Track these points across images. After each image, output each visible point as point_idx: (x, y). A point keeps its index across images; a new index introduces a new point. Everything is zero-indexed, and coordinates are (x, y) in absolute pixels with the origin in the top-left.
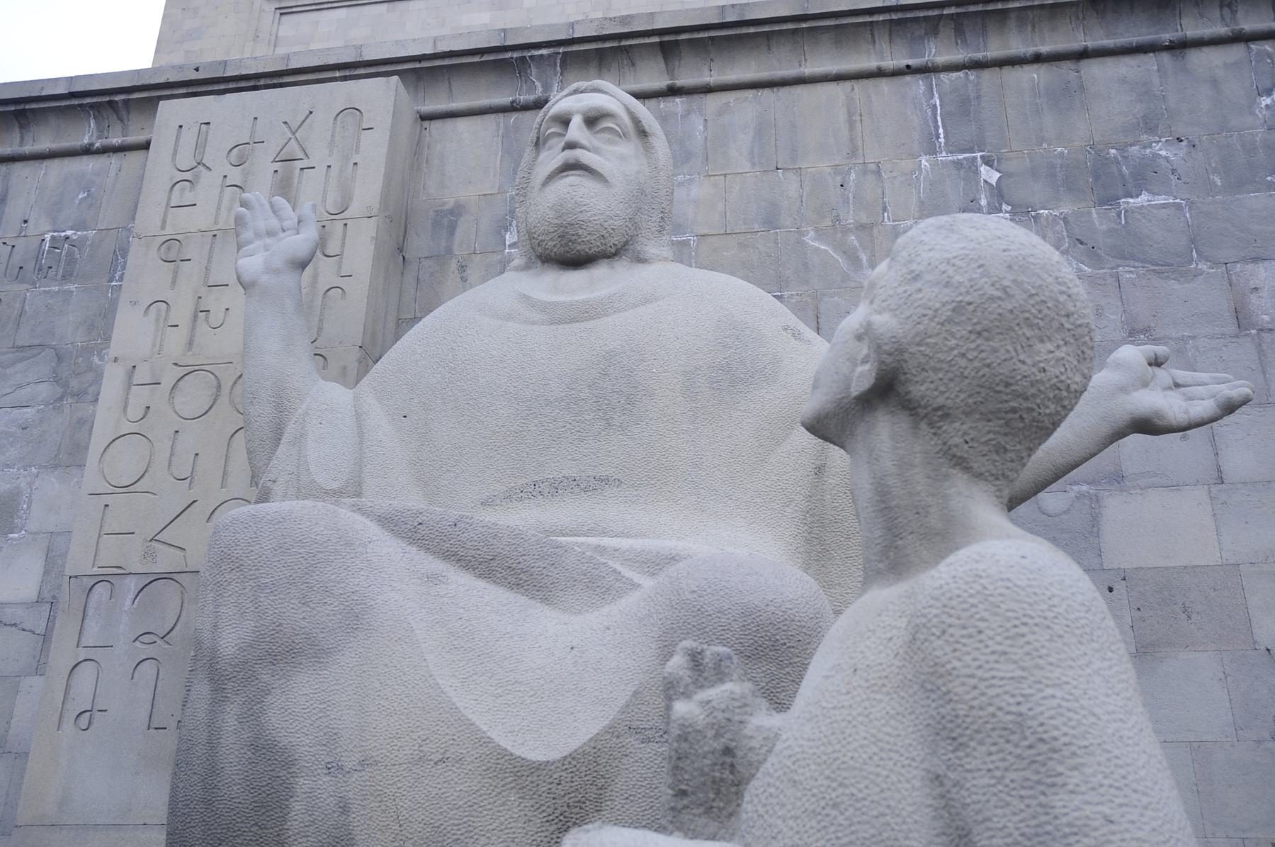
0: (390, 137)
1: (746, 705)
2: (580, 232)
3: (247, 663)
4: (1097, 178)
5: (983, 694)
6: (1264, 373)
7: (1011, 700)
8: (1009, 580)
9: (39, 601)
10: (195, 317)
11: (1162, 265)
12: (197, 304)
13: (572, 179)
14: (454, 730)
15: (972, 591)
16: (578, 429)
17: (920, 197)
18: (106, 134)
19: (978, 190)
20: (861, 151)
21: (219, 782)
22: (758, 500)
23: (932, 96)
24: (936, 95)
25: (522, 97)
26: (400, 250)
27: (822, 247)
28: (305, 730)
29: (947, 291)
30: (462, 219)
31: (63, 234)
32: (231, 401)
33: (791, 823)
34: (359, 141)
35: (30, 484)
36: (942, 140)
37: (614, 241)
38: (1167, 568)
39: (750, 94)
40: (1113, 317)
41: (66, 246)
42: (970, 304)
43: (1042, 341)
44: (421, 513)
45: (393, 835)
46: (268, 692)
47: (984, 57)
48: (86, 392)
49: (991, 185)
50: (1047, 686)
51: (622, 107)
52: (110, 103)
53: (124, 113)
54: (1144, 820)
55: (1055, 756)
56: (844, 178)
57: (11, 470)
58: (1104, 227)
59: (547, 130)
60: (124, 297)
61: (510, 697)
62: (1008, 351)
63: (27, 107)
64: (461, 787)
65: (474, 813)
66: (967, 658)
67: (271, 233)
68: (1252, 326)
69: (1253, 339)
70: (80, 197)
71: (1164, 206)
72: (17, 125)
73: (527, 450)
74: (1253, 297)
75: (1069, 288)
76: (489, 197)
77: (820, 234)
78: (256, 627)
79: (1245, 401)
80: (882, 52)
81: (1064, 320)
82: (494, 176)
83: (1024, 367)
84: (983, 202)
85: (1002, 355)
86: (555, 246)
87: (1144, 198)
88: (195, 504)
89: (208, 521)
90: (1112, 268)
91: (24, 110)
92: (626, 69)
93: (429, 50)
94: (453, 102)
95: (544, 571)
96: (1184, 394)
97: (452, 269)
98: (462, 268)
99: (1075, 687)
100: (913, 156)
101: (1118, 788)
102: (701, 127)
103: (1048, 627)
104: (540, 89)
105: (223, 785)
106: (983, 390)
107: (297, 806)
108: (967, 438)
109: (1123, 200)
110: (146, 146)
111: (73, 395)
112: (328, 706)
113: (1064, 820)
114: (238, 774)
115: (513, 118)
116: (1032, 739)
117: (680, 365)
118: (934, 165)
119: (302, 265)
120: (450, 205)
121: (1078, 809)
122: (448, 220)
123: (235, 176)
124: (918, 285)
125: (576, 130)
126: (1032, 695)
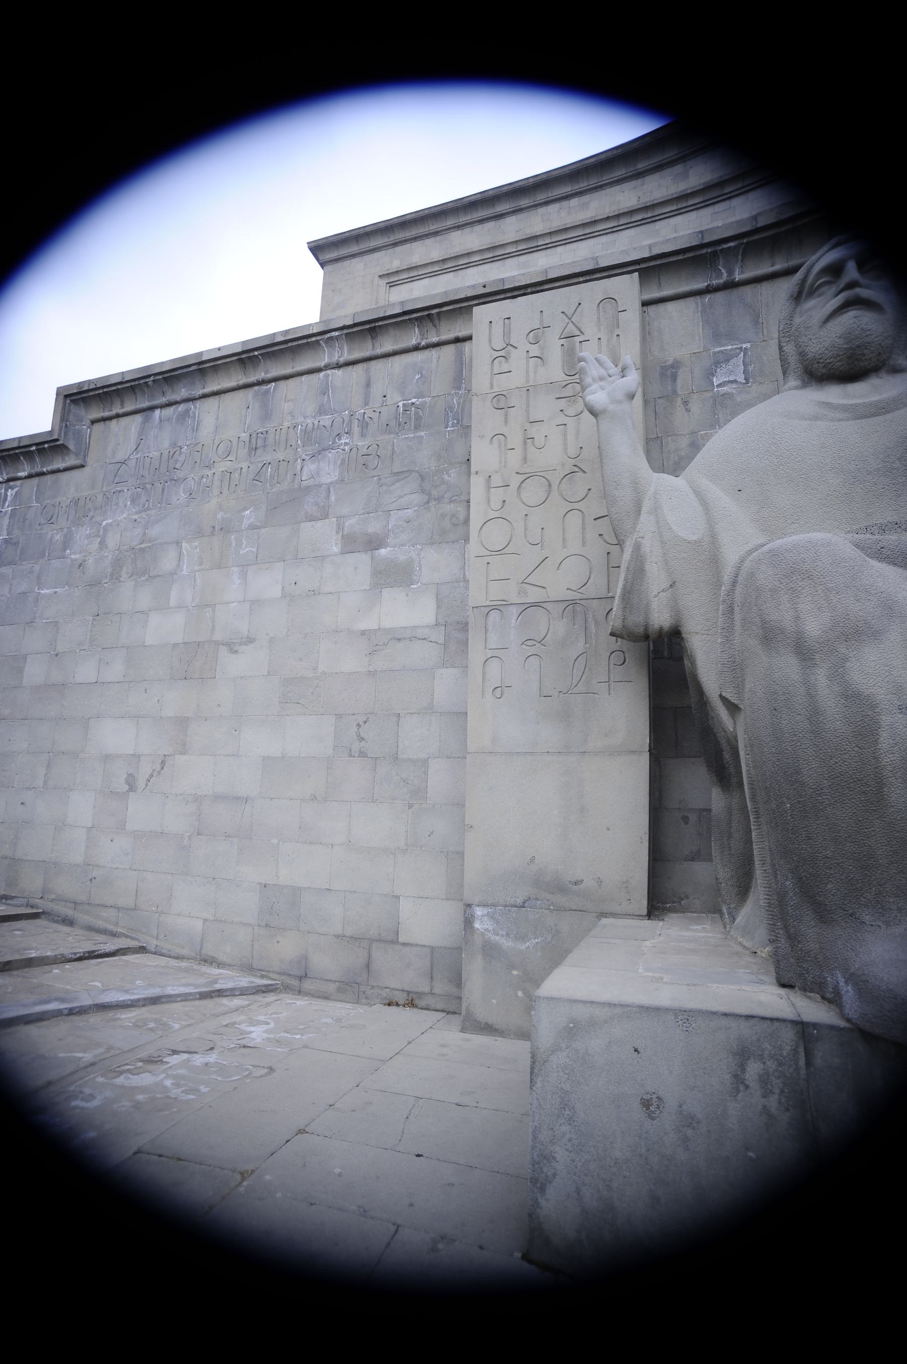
3: (829, 641)
10: (525, 443)
16: (895, 489)
18: (426, 336)
21: (823, 719)
32: (561, 494)
35: (418, 555)
41: (413, 409)
44: (880, 541)
46: (846, 659)
48: (443, 497)
52: (429, 315)
53: (437, 321)
63: (377, 324)
67: (601, 379)
70: (416, 377)
72: (370, 337)
73: (857, 505)
76: (698, 354)
78: (832, 616)
82: (699, 340)
89: (558, 569)
91: (375, 327)
93: (646, 254)
94: (662, 291)
97: (678, 404)
98: (686, 403)
105: (828, 721)
110: (470, 338)
111: (435, 500)
112: (891, 668)
114: (838, 714)
115: (707, 298)
120: (671, 362)
123: (535, 350)
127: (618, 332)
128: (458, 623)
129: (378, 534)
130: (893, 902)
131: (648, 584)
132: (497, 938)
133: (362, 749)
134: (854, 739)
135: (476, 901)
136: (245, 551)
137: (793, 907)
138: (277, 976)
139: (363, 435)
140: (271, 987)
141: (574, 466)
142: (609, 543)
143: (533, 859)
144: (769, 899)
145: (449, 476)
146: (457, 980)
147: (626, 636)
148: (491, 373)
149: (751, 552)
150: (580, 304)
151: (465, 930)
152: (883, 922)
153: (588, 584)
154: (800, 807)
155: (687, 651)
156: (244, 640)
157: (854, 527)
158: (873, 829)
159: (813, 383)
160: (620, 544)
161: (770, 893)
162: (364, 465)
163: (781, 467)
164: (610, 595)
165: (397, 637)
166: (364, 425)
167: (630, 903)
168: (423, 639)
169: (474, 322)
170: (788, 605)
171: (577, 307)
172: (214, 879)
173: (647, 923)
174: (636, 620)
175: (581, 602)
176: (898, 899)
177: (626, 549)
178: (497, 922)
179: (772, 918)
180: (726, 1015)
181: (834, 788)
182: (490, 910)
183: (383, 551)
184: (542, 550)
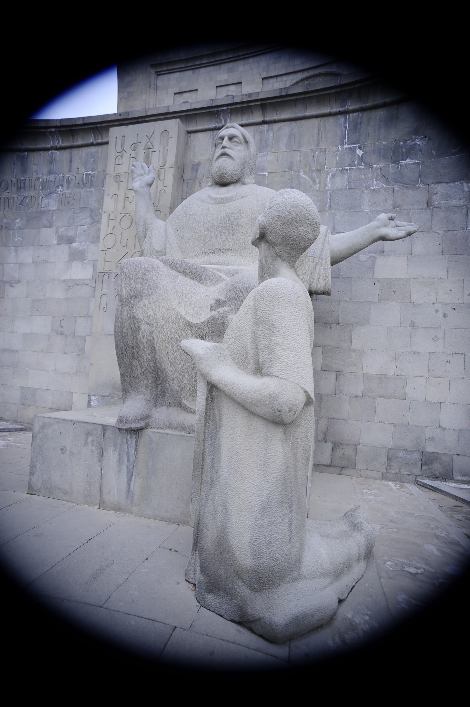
0: (177, 140)
1: (228, 313)
2: (225, 176)
5: (263, 314)
6: (431, 221)
7: (268, 316)
8: (272, 288)
10: (125, 199)
11: (408, 185)
12: (125, 195)
13: (224, 158)
15: (264, 290)
17: (337, 160)
20: (320, 144)
25: (218, 125)
26: (182, 177)
28: (142, 314)
29: (277, 212)
30: (200, 167)
31: (89, 173)
33: (230, 340)
34: (168, 142)
35: (87, 247)
36: (346, 140)
37: (236, 178)
38: (391, 279)
39: (288, 123)
40: (389, 202)
41: (90, 176)
42: (281, 216)
43: (300, 226)
50: (276, 313)
51: (240, 133)
54: (291, 343)
55: (275, 328)
56: (314, 154)
58: (393, 171)
59: (218, 141)
60: (106, 194)
61: (190, 307)
62: (290, 229)
66: (261, 305)
67: (141, 175)
69: (431, 210)
70: (92, 160)
74: (434, 196)
75: (310, 212)
77: (305, 173)
79: (415, 232)
81: (307, 221)
83: (295, 233)
84: (356, 162)
85: (289, 230)
86: (218, 180)
96: (398, 229)
98: (200, 183)
99: (282, 314)
101: (286, 336)
102: (272, 136)
103: (279, 300)
106: (284, 239)
107: (141, 332)
108: (281, 251)
109: (401, 162)
113: (274, 342)
116: (270, 324)
117: (251, 217)
118: (343, 149)
119: (150, 185)
120: (196, 162)
121: (277, 340)
122: (196, 167)
123: (133, 154)
124: (271, 210)
125: (226, 142)
126: (272, 315)
127: (167, 148)
135: (92, 394)
136: (17, 240)
138: (26, 425)
139: (68, 188)
140: (24, 429)
148: (115, 164)
156: (16, 281)
166: (69, 182)
172: (3, 385)
180: (84, 422)
182: (97, 398)
183: (74, 245)
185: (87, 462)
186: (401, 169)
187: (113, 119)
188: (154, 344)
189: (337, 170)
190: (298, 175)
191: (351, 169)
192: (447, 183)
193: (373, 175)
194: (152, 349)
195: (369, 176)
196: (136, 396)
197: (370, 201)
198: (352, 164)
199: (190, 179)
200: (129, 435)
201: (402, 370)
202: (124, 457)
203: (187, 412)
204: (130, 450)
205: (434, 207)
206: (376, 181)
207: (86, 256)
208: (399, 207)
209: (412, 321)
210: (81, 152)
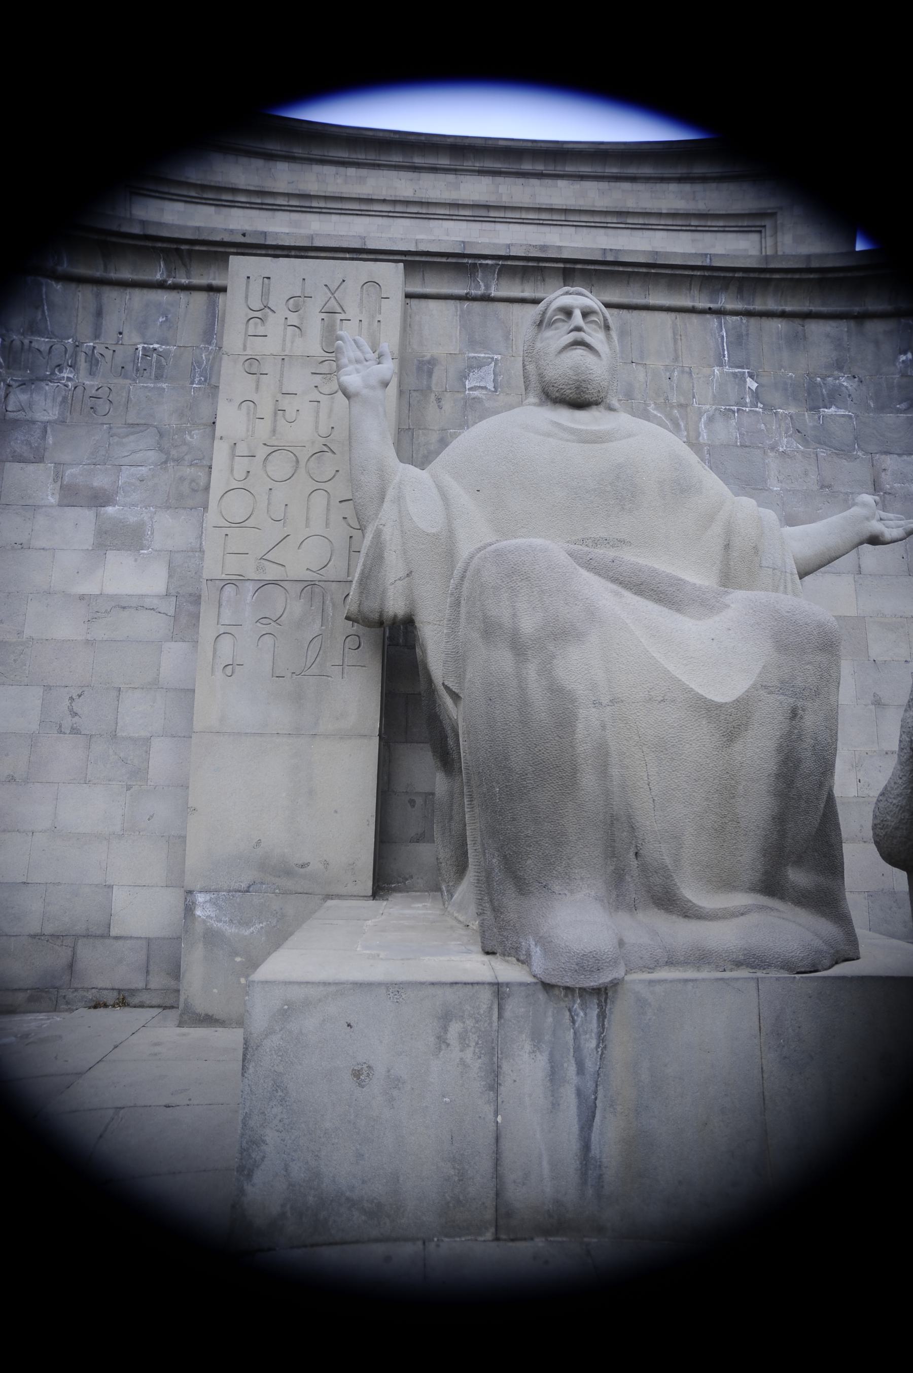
2: (589, 386)
4: (809, 394)
9: (168, 595)
10: (275, 414)
13: (579, 352)
14: (669, 684)
19: (745, 393)
20: (680, 358)
22: (700, 561)
23: (721, 330)
24: (724, 330)
27: (659, 415)
28: (579, 681)
30: (437, 368)
31: (151, 346)
32: (308, 473)
35: (151, 518)
40: (813, 477)
45: (635, 743)
46: (553, 657)
47: (754, 309)
48: (183, 459)
49: (752, 390)
56: (671, 374)
57: (136, 508)
64: (675, 716)
65: (683, 731)
67: (358, 361)
68: (881, 490)
70: (161, 320)
71: (843, 416)
73: (577, 519)
74: (883, 474)
77: (658, 407)
80: (694, 297)
82: (456, 342)
84: (748, 400)
87: (832, 410)
88: (288, 537)
89: (299, 548)
90: (814, 449)
92: (539, 283)
95: (673, 594)
96: (884, 524)
97: (432, 400)
98: (439, 400)
100: (710, 366)
104: (483, 288)
107: (580, 726)
111: (174, 460)
115: (466, 304)
118: (722, 373)
120: (428, 357)
123: (294, 319)
127: (379, 318)
128: (190, 595)
129: (106, 490)
130: (578, 873)
131: (386, 571)
132: (220, 925)
133: (75, 725)
134: (556, 729)
135: (198, 887)
137: (498, 883)
141: (324, 445)
142: (352, 527)
143: (259, 842)
144: (478, 876)
145: (192, 437)
146: (176, 971)
147: (361, 621)
149: (480, 550)
150: (344, 281)
151: (185, 918)
152: (569, 890)
153: (328, 565)
154: (507, 791)
155: (419, 640)
157: (573, 538)
158: (566, 810)
159: (549, 403)
160: (362, 529)
161: (479, 871)
162: (92, 408)
163: (516, 474)
164: (350, 579)
165: (120, 604)
167: (356, 885)
168: (151, 609)
169: (230, 273)
170: (507, 603)
171: (341, 284)
173: (372, 903)
174: (371, 606)
175: (320, 583)
176: (581, 869)
177: (367, 535)
178: (220, 908)
179: (481, 894)
180: (433, 984)
181: (537, 774)
182: (212, 896)
183: (110, 510)
184: (284, 526)
185: (447, 1100)
186: (825, 423)
187: (225, 240)
188: (607, 754)
189: (716, 409)
190: (646, 410)
191: (741, 411)
192: (900, 455)
193: (780, 426)
194: (603, 771)
195: (774, 428)
196: (572, 892)
197: (779, 472)
198: (741, 403)
199: (414, 390)
200: (579, 1001)
201: (869, 786)
202: (565, 1065)
203: (686, 916)
204: (582, 1042)
205: (885, 493)
206: (786, 437)
207: (148, 540)
208: (829, 486)
209: (875, 695)
210: (128, 297)
